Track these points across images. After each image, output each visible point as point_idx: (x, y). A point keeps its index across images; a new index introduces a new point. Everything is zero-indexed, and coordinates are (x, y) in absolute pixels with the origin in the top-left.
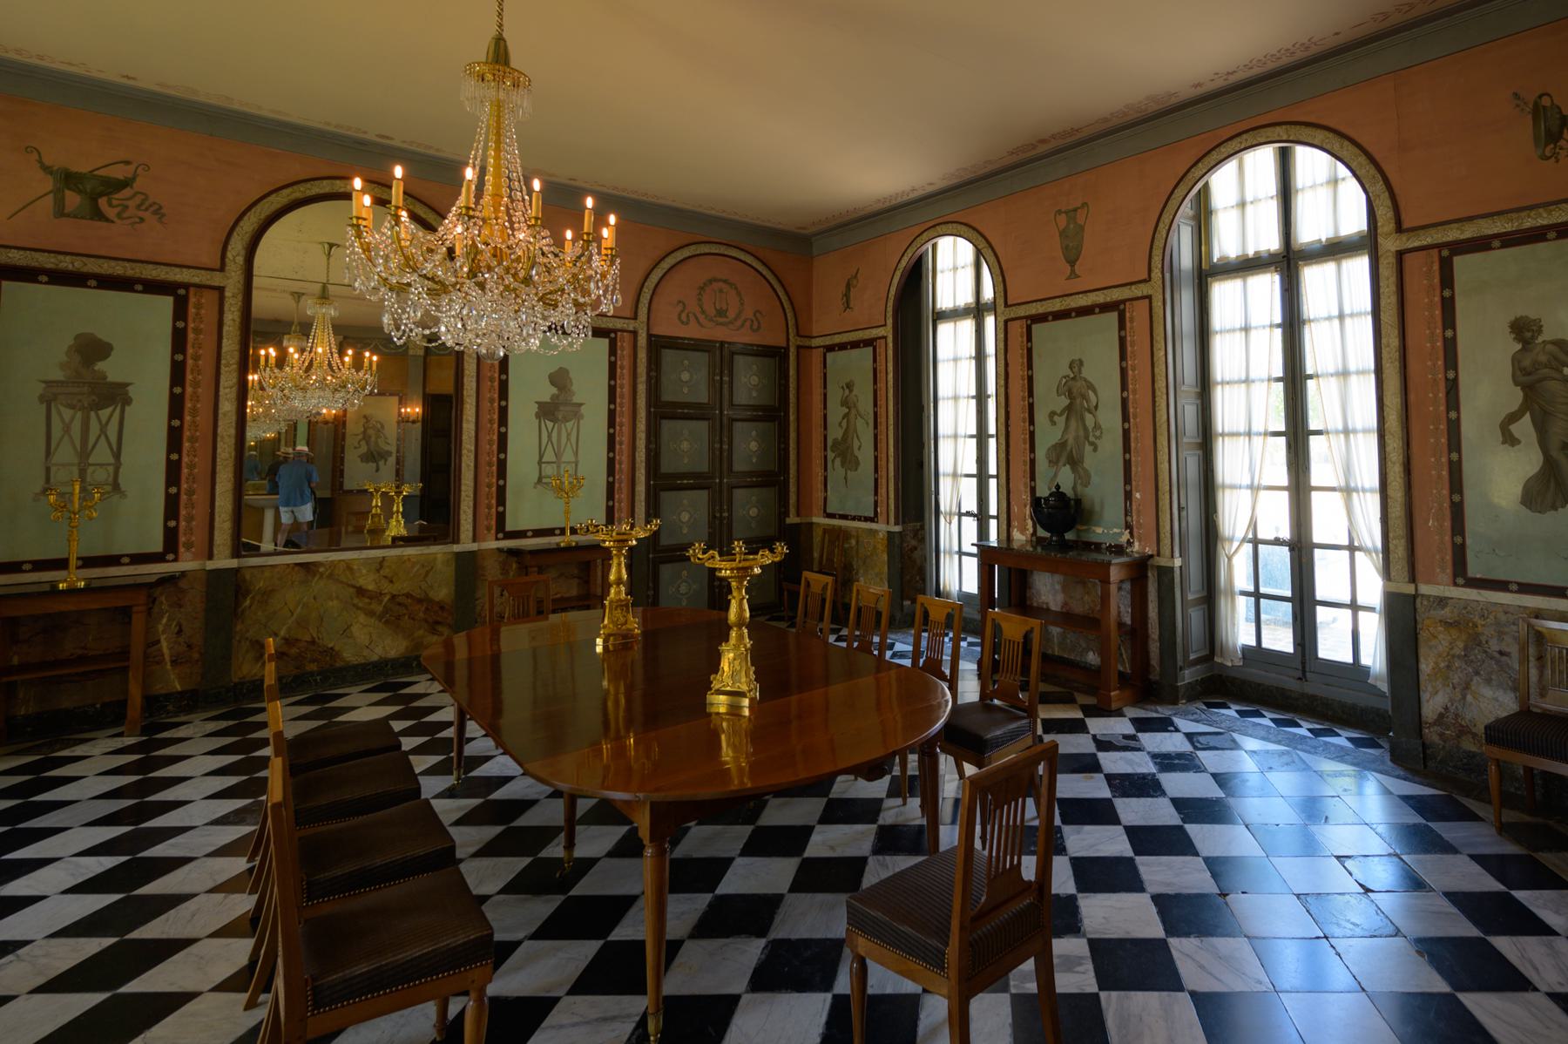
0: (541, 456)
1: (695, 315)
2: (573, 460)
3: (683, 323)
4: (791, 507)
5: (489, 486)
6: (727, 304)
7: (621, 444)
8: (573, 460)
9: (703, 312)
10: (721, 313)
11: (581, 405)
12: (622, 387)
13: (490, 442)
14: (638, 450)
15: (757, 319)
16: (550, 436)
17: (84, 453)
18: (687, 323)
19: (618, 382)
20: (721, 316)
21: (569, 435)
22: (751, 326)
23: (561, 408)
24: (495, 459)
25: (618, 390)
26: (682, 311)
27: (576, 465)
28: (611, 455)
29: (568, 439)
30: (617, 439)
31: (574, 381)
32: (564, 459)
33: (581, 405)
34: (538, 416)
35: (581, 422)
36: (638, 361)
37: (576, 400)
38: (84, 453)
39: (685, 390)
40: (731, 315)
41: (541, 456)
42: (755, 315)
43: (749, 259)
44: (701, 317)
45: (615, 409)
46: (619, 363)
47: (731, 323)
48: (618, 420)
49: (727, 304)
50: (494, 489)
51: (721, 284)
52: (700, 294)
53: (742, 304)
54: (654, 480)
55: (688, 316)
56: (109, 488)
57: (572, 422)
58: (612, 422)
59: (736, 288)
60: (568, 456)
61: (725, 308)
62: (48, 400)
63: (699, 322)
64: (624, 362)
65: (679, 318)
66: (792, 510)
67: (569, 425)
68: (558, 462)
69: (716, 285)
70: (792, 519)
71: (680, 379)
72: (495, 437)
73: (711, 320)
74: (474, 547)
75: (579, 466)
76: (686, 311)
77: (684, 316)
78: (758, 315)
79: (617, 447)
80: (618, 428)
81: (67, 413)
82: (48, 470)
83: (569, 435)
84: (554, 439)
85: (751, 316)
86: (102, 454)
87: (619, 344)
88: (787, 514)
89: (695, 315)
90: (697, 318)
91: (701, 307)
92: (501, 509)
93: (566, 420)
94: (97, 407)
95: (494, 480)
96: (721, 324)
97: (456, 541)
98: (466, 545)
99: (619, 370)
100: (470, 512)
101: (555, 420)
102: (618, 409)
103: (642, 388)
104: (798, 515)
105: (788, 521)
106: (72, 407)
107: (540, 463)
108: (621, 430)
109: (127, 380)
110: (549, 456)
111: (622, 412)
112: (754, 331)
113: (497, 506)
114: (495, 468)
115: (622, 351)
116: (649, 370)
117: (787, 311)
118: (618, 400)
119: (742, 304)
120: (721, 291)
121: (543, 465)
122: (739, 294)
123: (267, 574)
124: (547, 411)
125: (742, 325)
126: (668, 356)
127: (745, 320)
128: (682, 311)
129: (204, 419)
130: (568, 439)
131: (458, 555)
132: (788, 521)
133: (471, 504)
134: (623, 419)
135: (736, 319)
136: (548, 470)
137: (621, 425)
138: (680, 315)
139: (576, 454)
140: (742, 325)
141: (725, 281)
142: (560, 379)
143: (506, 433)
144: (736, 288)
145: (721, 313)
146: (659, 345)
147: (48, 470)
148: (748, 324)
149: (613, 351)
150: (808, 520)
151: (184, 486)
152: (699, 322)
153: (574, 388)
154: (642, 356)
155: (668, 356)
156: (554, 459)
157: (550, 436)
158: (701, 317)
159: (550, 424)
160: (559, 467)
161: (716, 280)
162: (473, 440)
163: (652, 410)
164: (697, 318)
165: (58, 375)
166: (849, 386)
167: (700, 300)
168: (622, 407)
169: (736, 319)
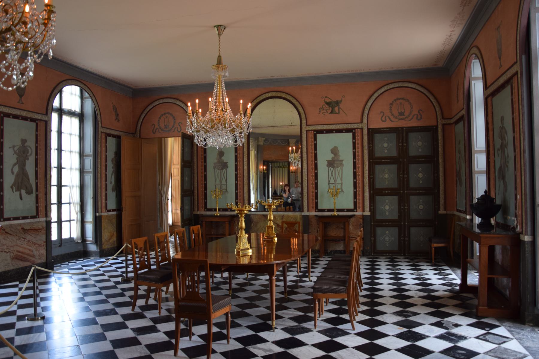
0: (329, 181)
1: (389, 117)
2: (341, 182)
3: (383, 121)
4: (441, 205)
5: (313, 192)
6: (404, 109)
7: (359, 176)
8: (341, 182)
9: (392, 115)
10: (401, 114)
11: (342, 160)
12: (358, 152)
13: (312, 176)
14: (365, 178)
15: (420, 114)
16: (332, 174)
17: (221, 181)
18: (385, 121)
19: (357, 150)
20: (401, 116)
21: (339, 173)
22: (417, 117)
23: (336, 162)
24: (314, 182)
25: (357, 153)
26: (383, 116)
27: (342, 185)
28: (355, 180)
29: (339, 174)
30: (357, 174)
31: (340, 151)
32: (337, 182)
33: (342, 160)
34: (327, 166)
35: (343, 167)
36: (364, 140)
37: (341, 158)
38: (221, 181)
39: (386, 151)
40: (406, 114)
41: (329, 181)
42: (419, 112)
43: (414, 86)
44: (392, 118)
45: (356, 162)
46: (357, 142)
47: (407, 117)
48: (357, 166)
49: (404, 109)
50: (314, 193)
51: (401, 101)
52: (391, 107)
53: (412, 108)
54: (373, 191)
55: (385, 118)
56: (225, 191)
57: (340, 168)
58: (355, 167)
59: (408, 101)
60: (339, 181)
61: (403, 111)
62: (214, 168)
63: (391, 120)
64: (359, 142)
65: (382, 120)
66: (442, 207)
67: (339, 169)
68: (335, 184)
69: (398, 102)
70: (442, 212)
71: (383, 146)
72: (314, 174)
73: (396, 118)
74: (307, 214)
75: (343, 185)
76: (384, 116)
77: (384, 119)
78: (420, 112)
79: (357, 177)
80: (357, 169)
81: (218, 171)
82: (215, 185)
83: (339, 173)
84: (334, 174)
85: (418, 114)
86: (224, 182)
87: (356, 134)
88: (439, 209)
89: (389, 117)
90: (390, 118)
91: (391, 113)
92: (316, 201)
93: (338, 167)
94: (222, 169)
95: (314, 190)
96: (402, 119)
97: (303, 211)
98: (306, 213)
99: (357, 145)
100: (306, 201)
101: (333, 167)
102: (357, 161)
103: (366, 152)
104: (445, 209)
105: (440, 212)
106: (218, 169)
107: (329, 184)
108: (358, 170)
109: (227, 162)
110: (332, 181)
111: (359, 162)
112: (418, 120)
113: (315, 200)
114: (314, 186)
115: (358, 137)
116: (369, 143)
117: (436, 107)
118: (357, 158)
119: (412, 108)
120: (401, 104)
121: (330, 185)
122: (410, 103)
123: (256, 217)
124: (331, 164)
125: (412, 118)
126: (377, 137)
127: (413, 116)
128: (383, 116)
129: (241, 171)
130: (339, 174)
131: (303, 216)
132: (440, 212)
133: (307, 198)
134: (359, 166)
135: (409, 116)
136: (332, 186)
137: (358, 168)
138: (382, 118)
139: (342, 180)
140: (412, 118)
141: (402, 99)
142: (335, 151)
143: (317, 173)
144: (408, 101)
145: (401, 114)
146: (372, 132)
147: (215, 185)
148: (416, 116)
149: (354, 137)
150: (451, 213)
151: (239, 190)
152: (391, 120)
153: (340, 154)
154: (366, 138)
155: (377, 137)
156: (334, 182)
157: (332, 174)
158: (392, 118)
159: (332, 169)
160: (335, 185)
161: (398, 99)
162: (306, 175)
163: (371, 161)
164: (390, 118)
165: (216, 161)
166: (460, 142)
167: (391, 110)
168: (358, 160)
169: (409, 116)
